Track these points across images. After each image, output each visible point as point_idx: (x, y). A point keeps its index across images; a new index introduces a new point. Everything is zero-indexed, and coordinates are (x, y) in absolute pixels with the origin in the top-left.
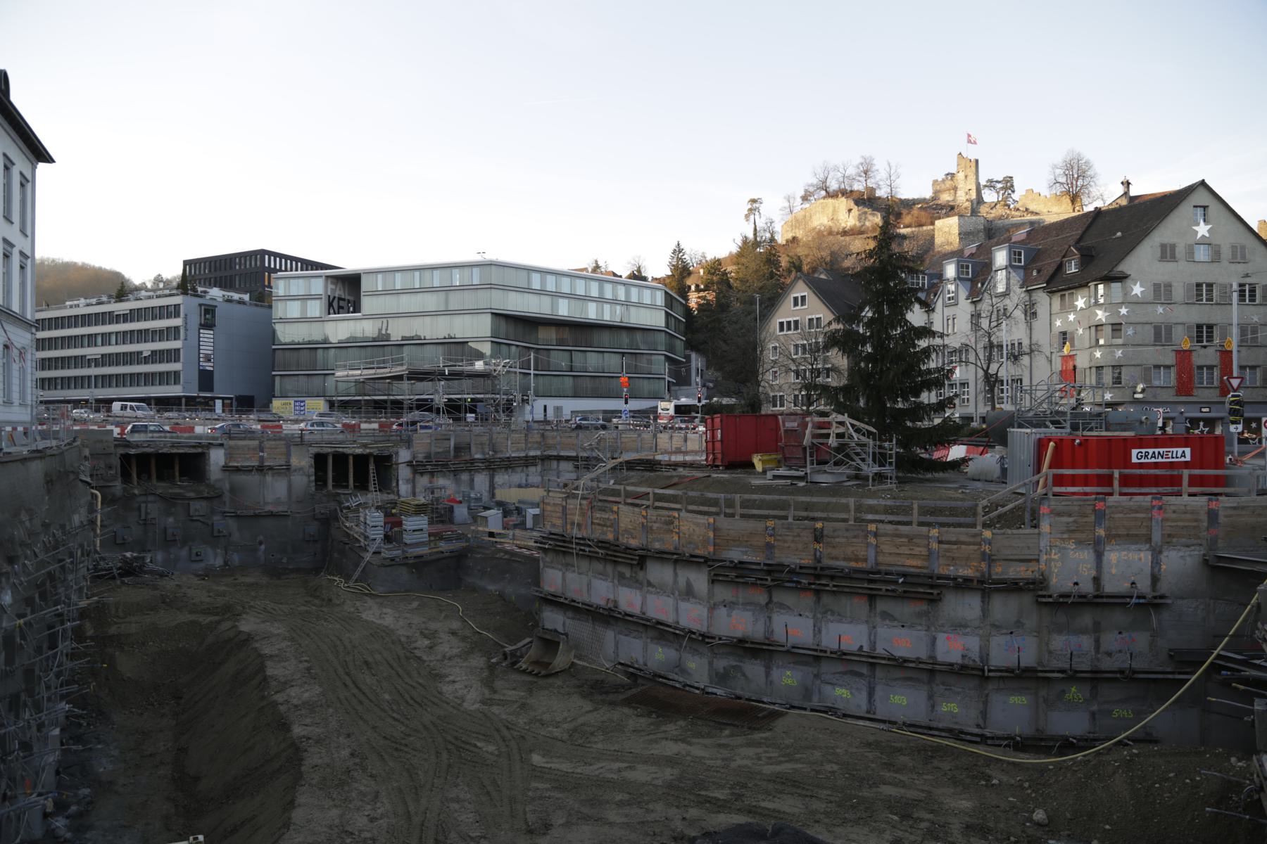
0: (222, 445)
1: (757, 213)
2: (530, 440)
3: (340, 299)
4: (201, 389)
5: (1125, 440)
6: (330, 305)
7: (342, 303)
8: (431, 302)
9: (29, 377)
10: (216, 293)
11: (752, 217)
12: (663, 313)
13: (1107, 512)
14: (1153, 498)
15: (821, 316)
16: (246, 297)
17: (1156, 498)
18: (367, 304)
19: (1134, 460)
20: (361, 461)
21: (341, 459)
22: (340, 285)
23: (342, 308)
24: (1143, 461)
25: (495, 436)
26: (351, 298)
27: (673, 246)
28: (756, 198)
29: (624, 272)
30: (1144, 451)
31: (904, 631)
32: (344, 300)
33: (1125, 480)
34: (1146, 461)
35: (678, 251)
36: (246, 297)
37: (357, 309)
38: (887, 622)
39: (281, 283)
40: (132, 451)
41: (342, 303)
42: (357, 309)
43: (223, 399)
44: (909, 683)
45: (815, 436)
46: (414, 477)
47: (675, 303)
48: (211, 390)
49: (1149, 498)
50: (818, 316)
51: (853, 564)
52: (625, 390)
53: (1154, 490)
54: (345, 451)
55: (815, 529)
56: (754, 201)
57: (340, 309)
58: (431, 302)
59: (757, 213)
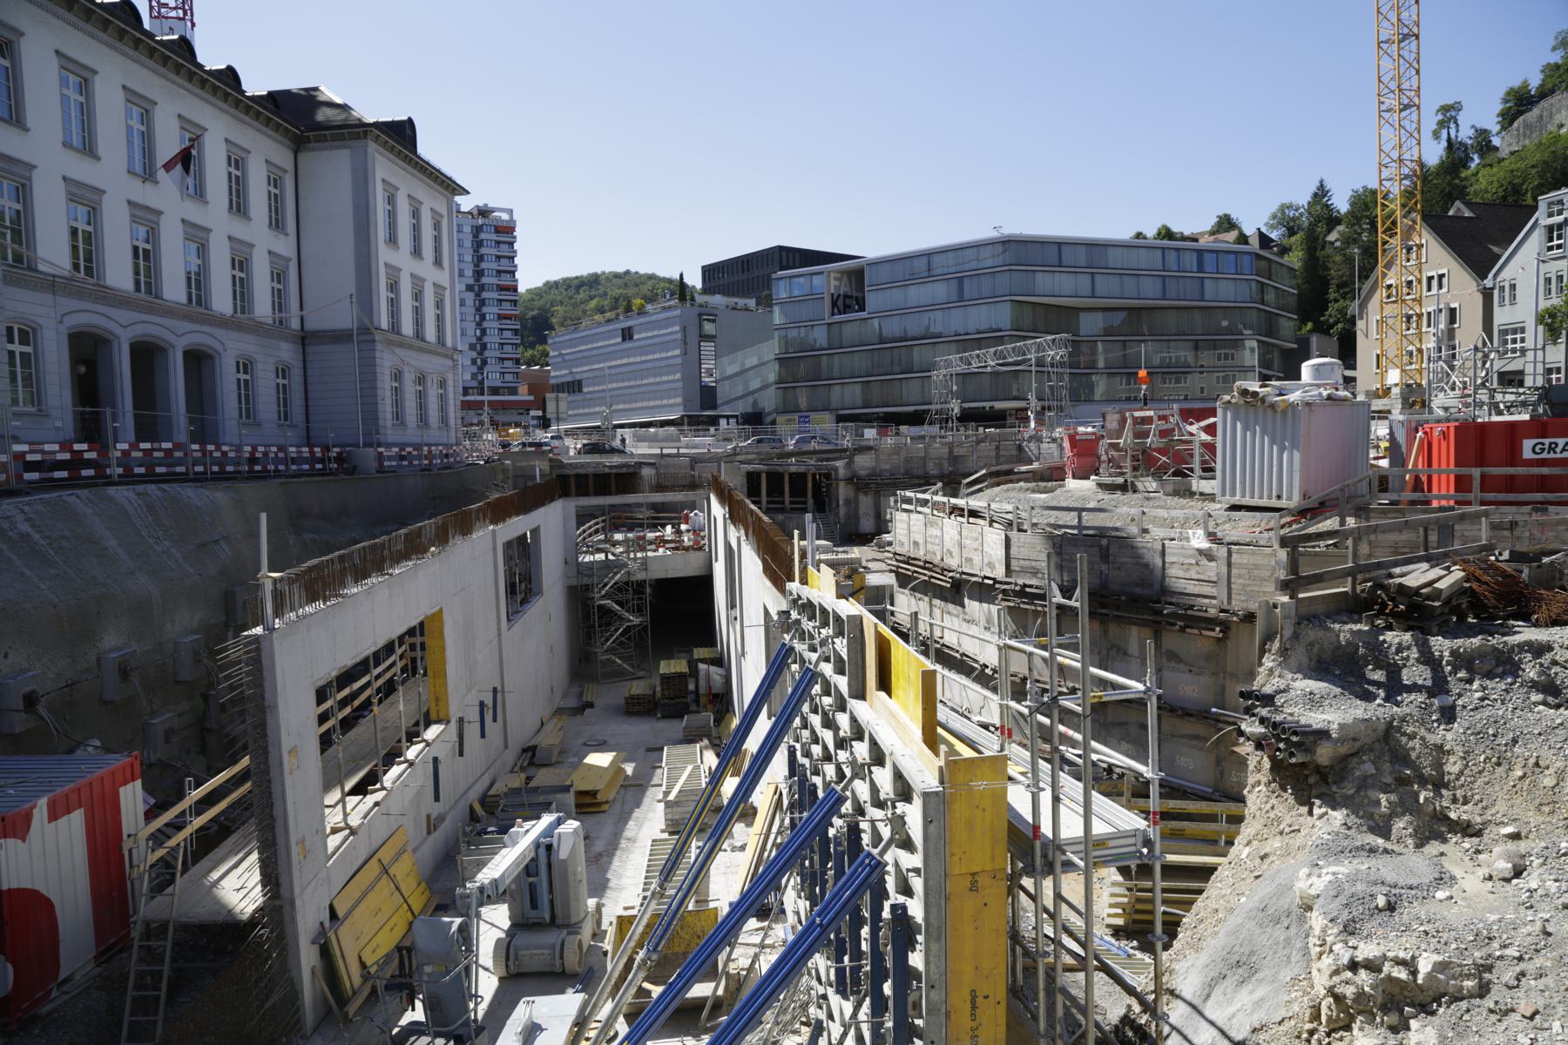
0: (653, 464)
1: (1452, 125)
2: (1002, 453)
3: (846, 296)
4: (703, 408)
5: (1512, 426)
6: (834, 304)
7: (848, 301)
8: (940, 291)
9: (451, 402)
10: (718, 300)
11: (1444, 132)
12: (1254, 284)
13: (1457, 527)
14: (1533, 509)
15: (1444, 271)
16: (752, 303)
17: (1536, 510)
18: (873, 300)
19: (1527, 453)
20: (798, 480)
21: (775, 478)
22: (845, 278)
23: (849, 307)
24: (1545, 455)
25: (956, 450)
26: (859, 295)
27: (1312, 188)
28: (1451, 102)
29: (1151, 232)
30: (1547, 441)
31: (1187, 676)
32: (851, 297)
33: (1487, 483)
34: (1552, 455)
35: (1321, 193)
36: (752, 303)
37: (862, 309)
38: (1173, 664)
39: (781, 283)
40: (567, 472)
41: (848, 301)
42: (862, 309)
43: (728, 417)
44: (1195, 742)
45: (1137, 435)
46: (856, 498)
47: (1274, 265)
48: (714, 407)
49: (1527, 509)
50: (1440, 272)
51: (1138, 590)
52: (1144, 387)
53: (1538, 496)
54: (780, 469)
55: (1101, 546)
56: (1445, 109)
57: (847, 309)
58: (940, 291)
59: (1452, 125)
